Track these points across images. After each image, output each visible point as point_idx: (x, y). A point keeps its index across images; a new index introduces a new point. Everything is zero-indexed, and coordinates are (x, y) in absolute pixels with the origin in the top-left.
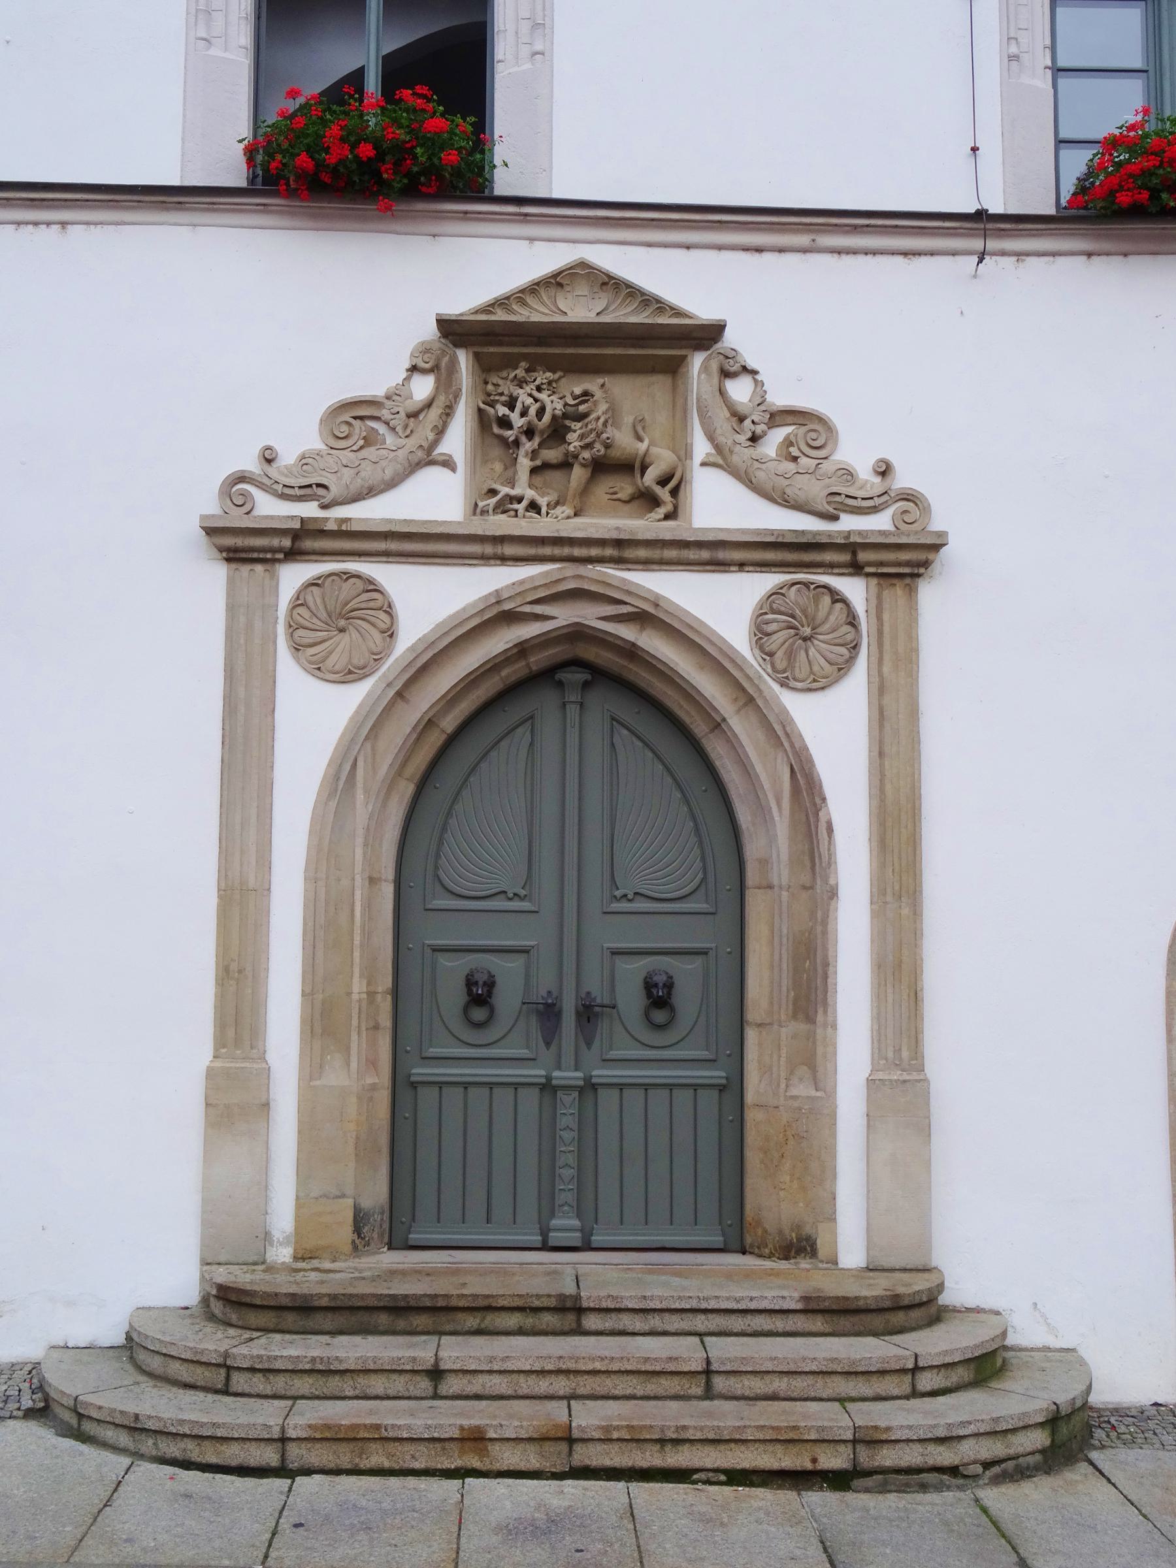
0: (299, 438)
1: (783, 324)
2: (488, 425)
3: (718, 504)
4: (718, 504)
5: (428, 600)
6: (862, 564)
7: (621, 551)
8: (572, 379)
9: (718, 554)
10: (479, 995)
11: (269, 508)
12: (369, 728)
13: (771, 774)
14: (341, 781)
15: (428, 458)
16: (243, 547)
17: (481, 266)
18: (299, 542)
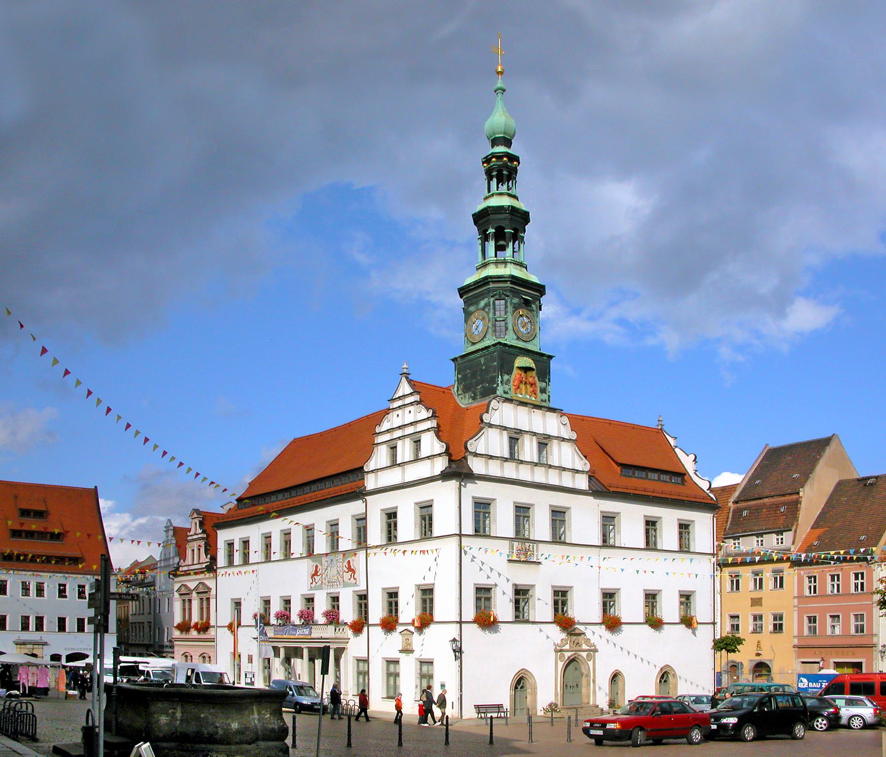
0: (559, 642)
1: (588, 631)
3: (584, 647)
5: (567, 655)
16: (556, 651)
18: (561, 651)
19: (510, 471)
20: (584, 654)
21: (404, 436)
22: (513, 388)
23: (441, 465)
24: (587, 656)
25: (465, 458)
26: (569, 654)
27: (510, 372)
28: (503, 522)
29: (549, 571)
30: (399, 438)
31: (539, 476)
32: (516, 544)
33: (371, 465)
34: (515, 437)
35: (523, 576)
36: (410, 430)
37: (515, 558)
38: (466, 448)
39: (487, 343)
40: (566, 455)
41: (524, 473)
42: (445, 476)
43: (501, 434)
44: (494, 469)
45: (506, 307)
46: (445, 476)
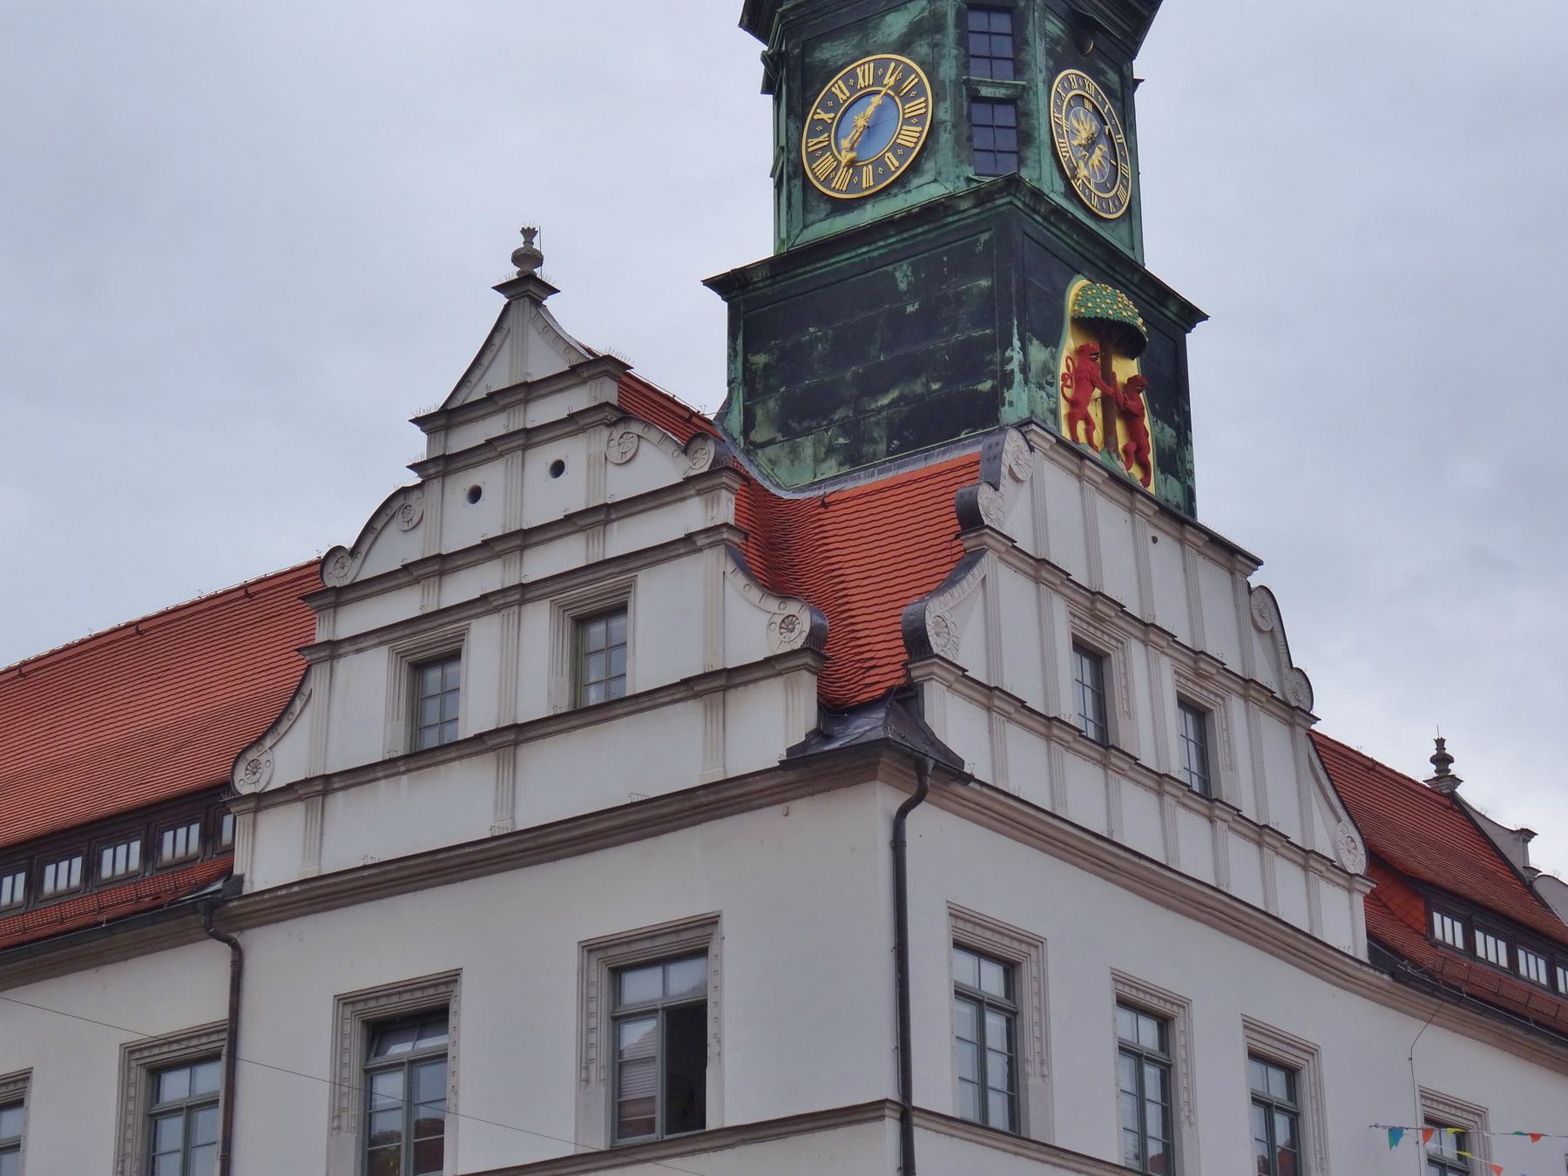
21: (524, 593)
22: (1064, 409)
23: (773, 724)
25: (906, 698)
27: (1052, 340)
30: (485, 604)
33: (288, 760)
36: (567, 555)
38: (917, 643)
39: (926, 191)
42: (811, 770)
45: (1019, 41)
46: (811, 770)
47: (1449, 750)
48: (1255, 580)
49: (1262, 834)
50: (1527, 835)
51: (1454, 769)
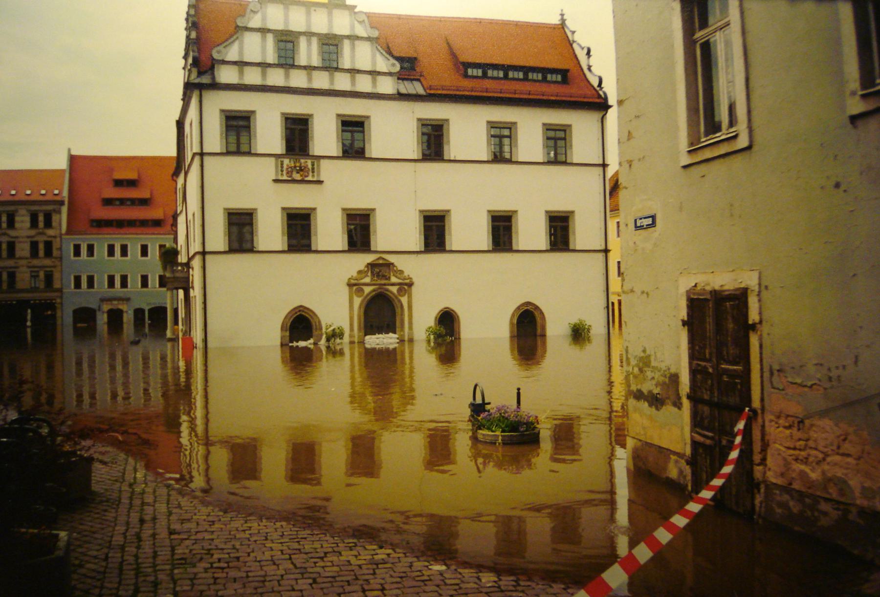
0: (355, 274)
2: (372, 272)
3: (394, 280)
4: (394, 280)
5: (367, 290)
6: (407, 286)
7: (385, 285)
8: (381, 269)
9: (393, 284)
10: (371, 326)
11: (353, 281)
12: (362, 301)
13: (399, 305)
14: (360, 307)
15: (367, 276)
16: (350, 285)
17: (370, 258)
19: (276, 78)
20: (394, 289)
24: (399, 290)
26: (371, 288)
28: (269, 135)
29: (337, 191)
31: (321, 81)
32: (286, 162)
34: (287, 40)
35: (299, 197)
37: (285, 178)
40: (364, 56)
41: (298, 79)
43: (264, 39)
44: (253, 77)
47: (564, 12)
48: (356, 10)
49: (354, 72)
50: (573, 32)
51: (565, 17)
